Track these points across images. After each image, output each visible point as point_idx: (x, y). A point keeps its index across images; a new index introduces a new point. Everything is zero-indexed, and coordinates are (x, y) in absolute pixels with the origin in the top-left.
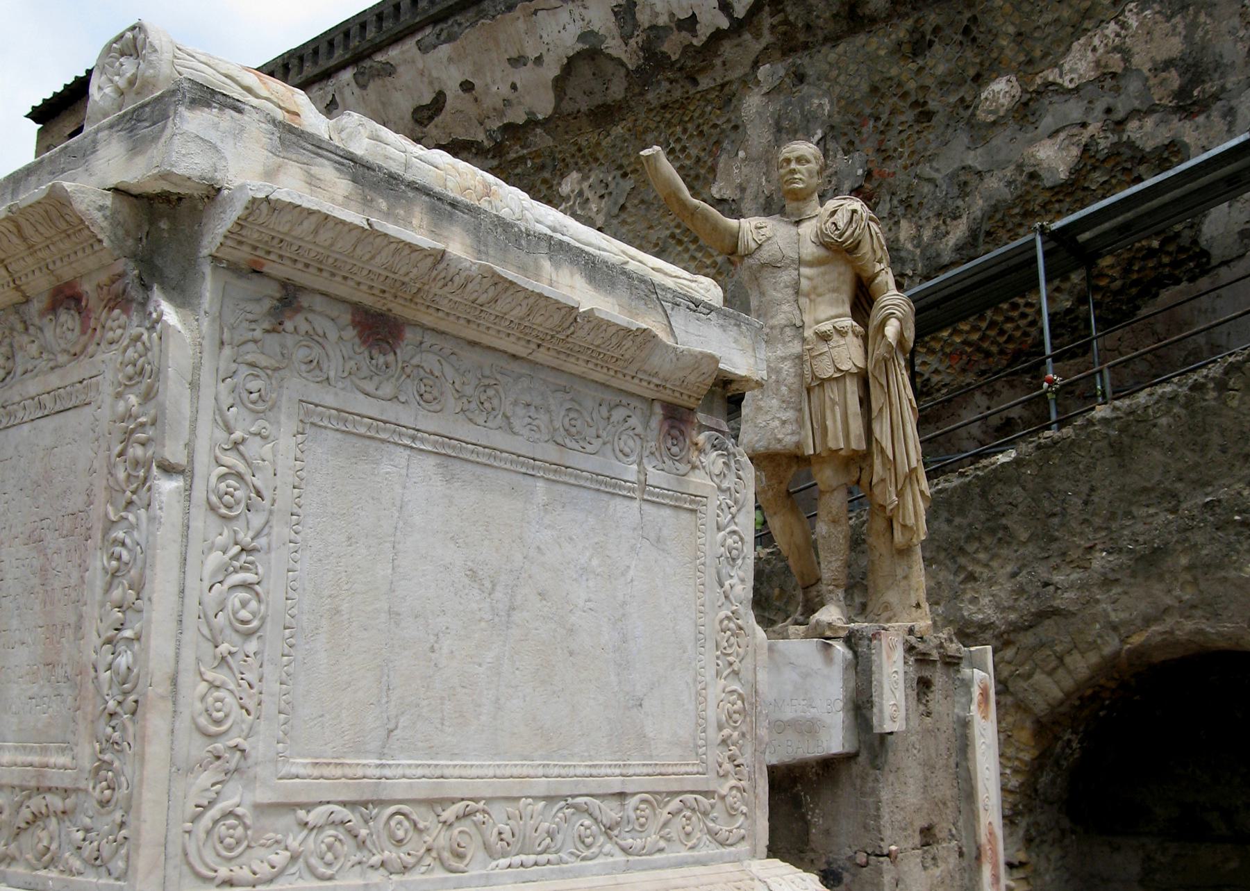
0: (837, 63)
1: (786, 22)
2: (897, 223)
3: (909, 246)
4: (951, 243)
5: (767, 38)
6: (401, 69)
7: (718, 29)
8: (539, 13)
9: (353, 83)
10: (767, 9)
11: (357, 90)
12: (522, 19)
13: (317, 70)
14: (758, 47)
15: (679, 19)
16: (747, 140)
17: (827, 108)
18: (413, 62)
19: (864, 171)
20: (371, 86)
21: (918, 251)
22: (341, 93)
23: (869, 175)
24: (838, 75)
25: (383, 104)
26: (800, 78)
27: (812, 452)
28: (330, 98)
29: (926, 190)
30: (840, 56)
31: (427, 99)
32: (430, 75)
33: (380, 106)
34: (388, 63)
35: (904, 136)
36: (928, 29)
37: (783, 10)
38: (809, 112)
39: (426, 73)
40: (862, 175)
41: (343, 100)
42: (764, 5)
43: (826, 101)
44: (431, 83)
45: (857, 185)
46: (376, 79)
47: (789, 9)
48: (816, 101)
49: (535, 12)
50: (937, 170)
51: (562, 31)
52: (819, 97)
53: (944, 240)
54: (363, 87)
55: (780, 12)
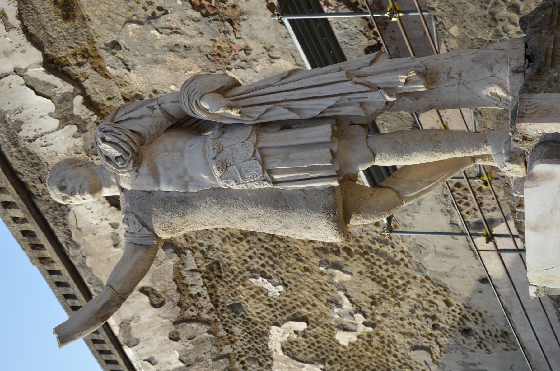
8: (79, 226)
51: (92, 210)
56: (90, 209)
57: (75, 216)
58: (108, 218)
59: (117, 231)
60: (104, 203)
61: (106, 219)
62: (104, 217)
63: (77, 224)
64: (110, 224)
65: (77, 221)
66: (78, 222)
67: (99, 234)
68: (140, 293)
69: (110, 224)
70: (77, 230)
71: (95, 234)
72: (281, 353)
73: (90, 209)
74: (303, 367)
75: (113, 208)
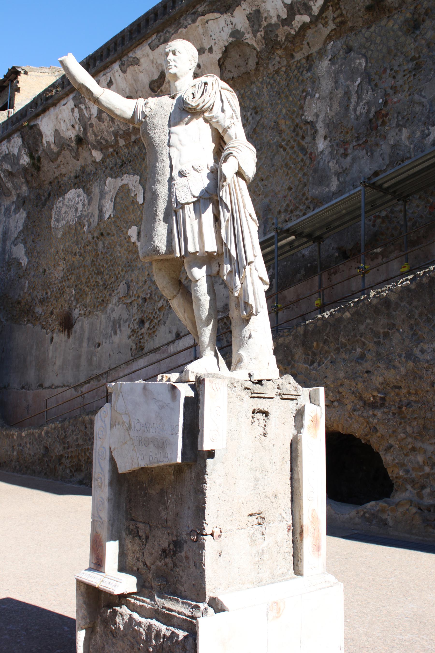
0: (370, 37)
1: (341, 15)
2: (400, 131)
3: (407, 143)
4: (431, 140)
5: (332, 26)
6: (142, 61)
7: (304, 23)
8: (210, 22)
9: (119, 70)
10: (330, 8)
11: (122, 74)
12: (200, 27)
13: (102, 64)
14: (326, 31)
15: (282, 19)
16: (320, 87)
17: (364, 65)
18: (148, 56)
19: (383, 101)
20: (128, 71)
21: (412, 146)
22: (114, 76)
23: (385, 103)
24: (371, 44)
25: (135, 80)
26: (349, 50)
27: (178, 255)
28: (109, 79)
29: (417, 109)
30: (372, 33)
31: (156, 77)
32: (157, 62)
33: (133, 82)
34: (135, 57)
35: (406, 78)
36: (423, 11)
37: (340, 8)
38: (354, 67)
39: (155, 61)
40: (382, 103)
41: (115, 80)
42: (328, 7)
43: (363, 61)
44: (157, 67)
45: (379, 109)
46: (130, 67)
47: (342, 7)
48: (358, 61)
49: (207, 22)
50: (424, 97)
51: (222, 32)
52: (359, 59)
53: (427, 138)
54: (124, 72)
55: (337, 9)
56: (222, 30)
57: (217, 18)
58: (216, 45)
59: (206, 52)
60: (228, 41)
61: (215, 43)
62: (216, 41)
63: (211, 20)
64: (212, 46)
65: (213, 20)
66: (212, 21)
67: (204, 38)
68: (160, 72)
69: (212, 46)
70: (206, 20)
71: (204, 35)
72: (120, 184)
73: (222, 30)
74: (111, 201)
75: (224, 49)
